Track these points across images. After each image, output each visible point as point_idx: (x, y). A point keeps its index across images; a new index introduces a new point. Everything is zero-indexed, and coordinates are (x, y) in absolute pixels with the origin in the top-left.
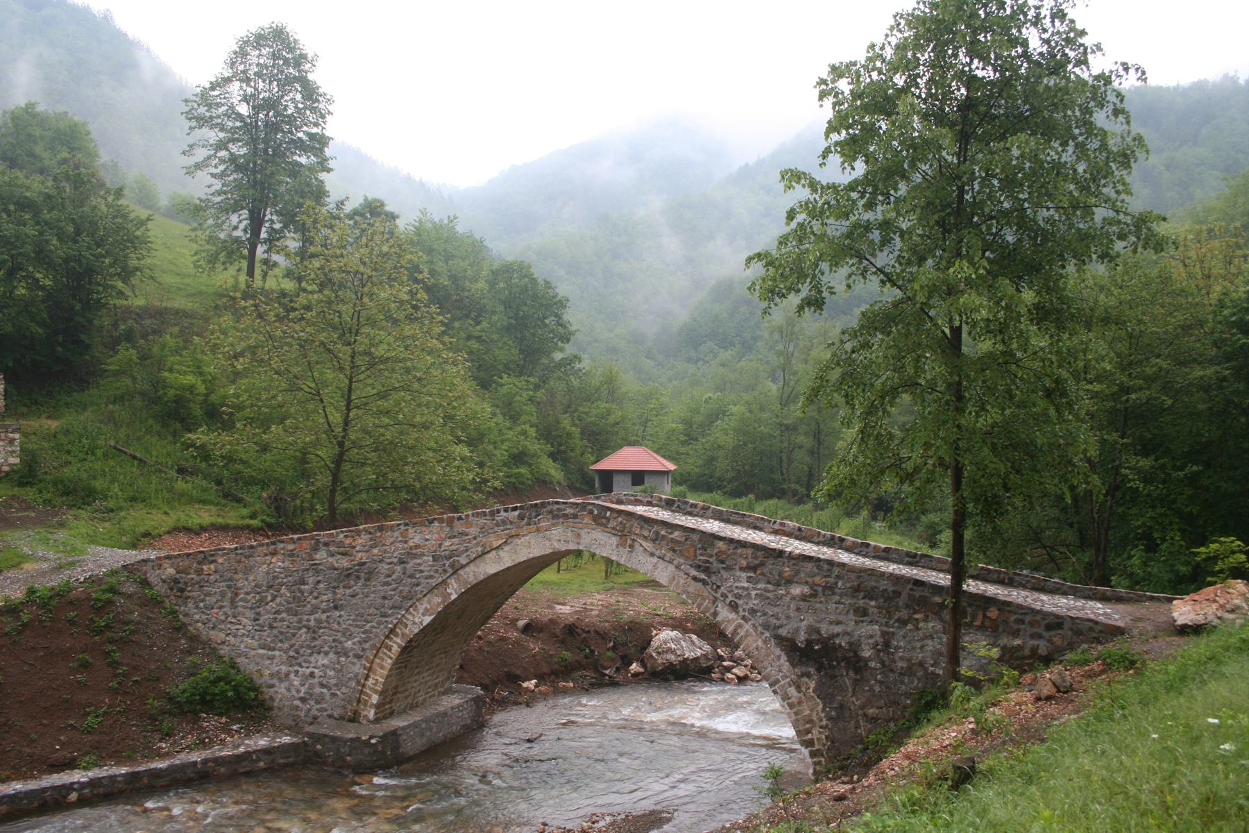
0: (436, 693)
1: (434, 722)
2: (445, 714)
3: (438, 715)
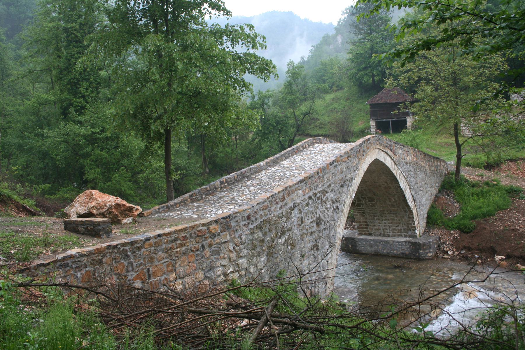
0: (403, 234)
1: (380, 243)
2: (387, 242)
3: (382, 241)
